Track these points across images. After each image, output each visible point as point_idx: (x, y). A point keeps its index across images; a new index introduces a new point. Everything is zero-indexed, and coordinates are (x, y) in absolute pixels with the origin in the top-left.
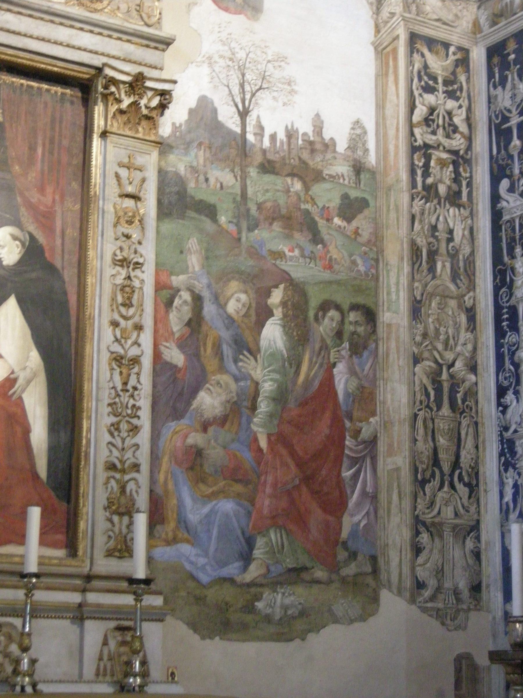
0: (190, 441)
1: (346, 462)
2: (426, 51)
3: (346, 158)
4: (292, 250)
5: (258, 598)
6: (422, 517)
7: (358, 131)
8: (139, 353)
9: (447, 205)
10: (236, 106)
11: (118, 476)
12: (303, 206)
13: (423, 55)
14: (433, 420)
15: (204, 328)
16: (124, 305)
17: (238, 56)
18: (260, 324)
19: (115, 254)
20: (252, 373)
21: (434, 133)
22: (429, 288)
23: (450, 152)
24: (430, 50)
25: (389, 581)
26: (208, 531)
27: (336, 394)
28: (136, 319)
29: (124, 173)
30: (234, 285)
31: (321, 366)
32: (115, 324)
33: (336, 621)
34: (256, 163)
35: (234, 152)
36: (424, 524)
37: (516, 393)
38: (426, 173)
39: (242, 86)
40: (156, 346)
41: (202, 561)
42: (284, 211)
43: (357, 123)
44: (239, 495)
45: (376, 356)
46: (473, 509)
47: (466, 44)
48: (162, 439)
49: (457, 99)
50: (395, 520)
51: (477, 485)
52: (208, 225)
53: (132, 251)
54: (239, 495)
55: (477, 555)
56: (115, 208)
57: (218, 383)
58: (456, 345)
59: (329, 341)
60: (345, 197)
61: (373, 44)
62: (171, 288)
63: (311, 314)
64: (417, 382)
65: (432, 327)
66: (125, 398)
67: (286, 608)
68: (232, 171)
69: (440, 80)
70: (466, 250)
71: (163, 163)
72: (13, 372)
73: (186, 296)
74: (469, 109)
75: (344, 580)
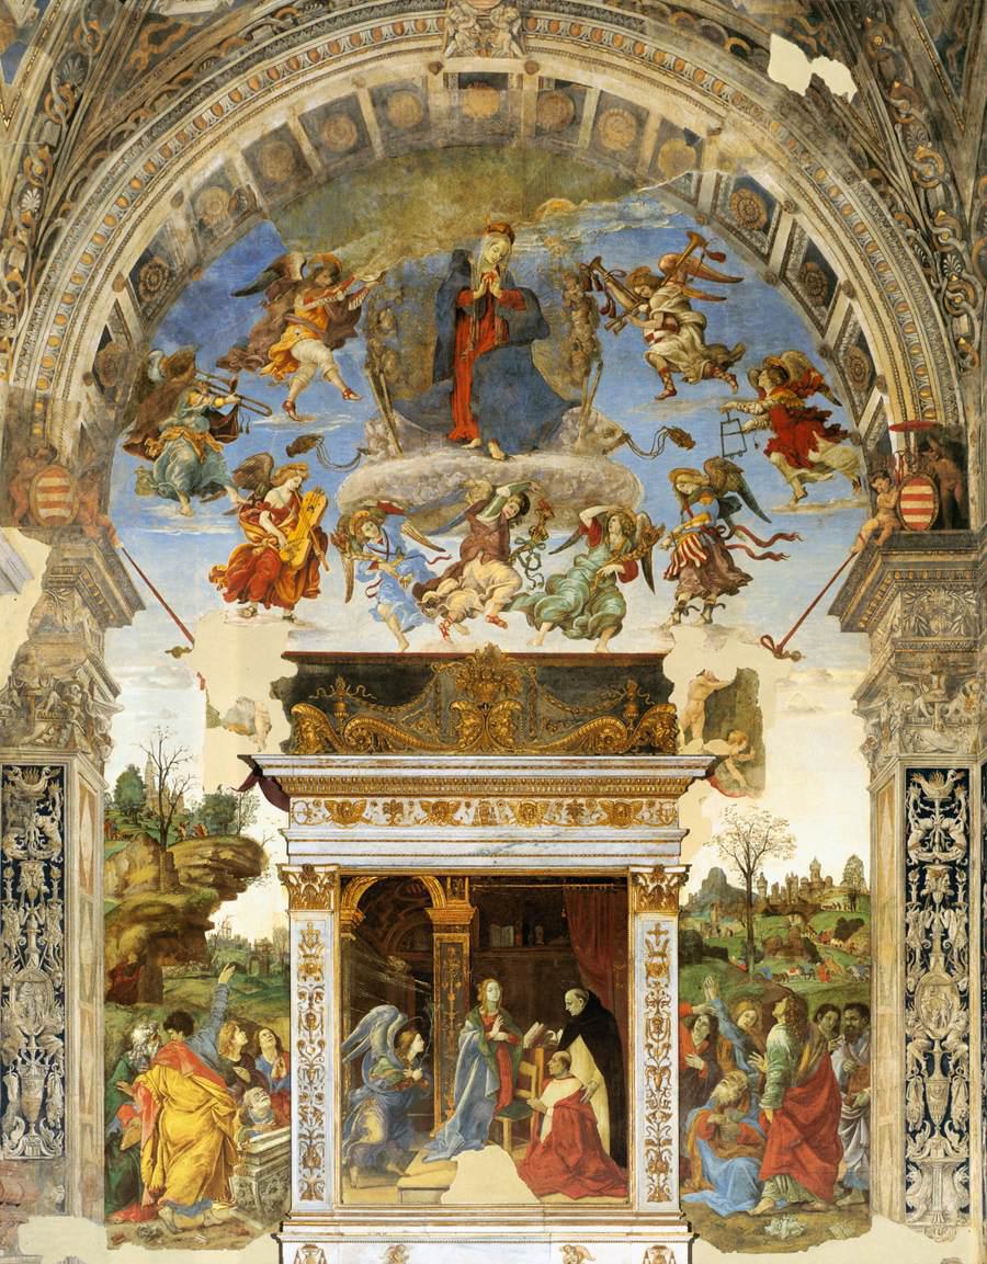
1: (842, 1123)
2: (922, 781)
6: (912, 1159)
7: (854, 866)
13: (919, 786)
15: (720, 1040)
21: (930, 851)
23: (945, 863)
24: (927, 780)
25: (880, 1207)
26: (726, 1182)
28: (666, 1040)
29: (652, 938)
30: (743, 1005)
32: (650, 1046)
33: (833, 1237)
34: (760, 910)
35: (741, 905)
36: (914, 1164)
38: (921, 886)
39: (748, 855)
40: (680, 1058)
41: (720, 1201)
42: (785, 942)
44: (750, 1154)
45: (870, 1041)
46: (962, 1150)
47: (965, 765)
48: (689, 1121)
49: (955, 816)
50: (887, 1161)
51: (968, 1131)
52: (721, 964)
54: (750, 1154)
55: (966, 1185)
57: (732, 1078)
60: (842, 921)
61: (868, 789)
63: (811, 1017)
64: (909, 1056)
66: (658, 1095)
69: (937, 804)
70: (962, 944)
71: (682, 926)
73: (705, 1019)
74: (968, 821)
75: (840, 1209)
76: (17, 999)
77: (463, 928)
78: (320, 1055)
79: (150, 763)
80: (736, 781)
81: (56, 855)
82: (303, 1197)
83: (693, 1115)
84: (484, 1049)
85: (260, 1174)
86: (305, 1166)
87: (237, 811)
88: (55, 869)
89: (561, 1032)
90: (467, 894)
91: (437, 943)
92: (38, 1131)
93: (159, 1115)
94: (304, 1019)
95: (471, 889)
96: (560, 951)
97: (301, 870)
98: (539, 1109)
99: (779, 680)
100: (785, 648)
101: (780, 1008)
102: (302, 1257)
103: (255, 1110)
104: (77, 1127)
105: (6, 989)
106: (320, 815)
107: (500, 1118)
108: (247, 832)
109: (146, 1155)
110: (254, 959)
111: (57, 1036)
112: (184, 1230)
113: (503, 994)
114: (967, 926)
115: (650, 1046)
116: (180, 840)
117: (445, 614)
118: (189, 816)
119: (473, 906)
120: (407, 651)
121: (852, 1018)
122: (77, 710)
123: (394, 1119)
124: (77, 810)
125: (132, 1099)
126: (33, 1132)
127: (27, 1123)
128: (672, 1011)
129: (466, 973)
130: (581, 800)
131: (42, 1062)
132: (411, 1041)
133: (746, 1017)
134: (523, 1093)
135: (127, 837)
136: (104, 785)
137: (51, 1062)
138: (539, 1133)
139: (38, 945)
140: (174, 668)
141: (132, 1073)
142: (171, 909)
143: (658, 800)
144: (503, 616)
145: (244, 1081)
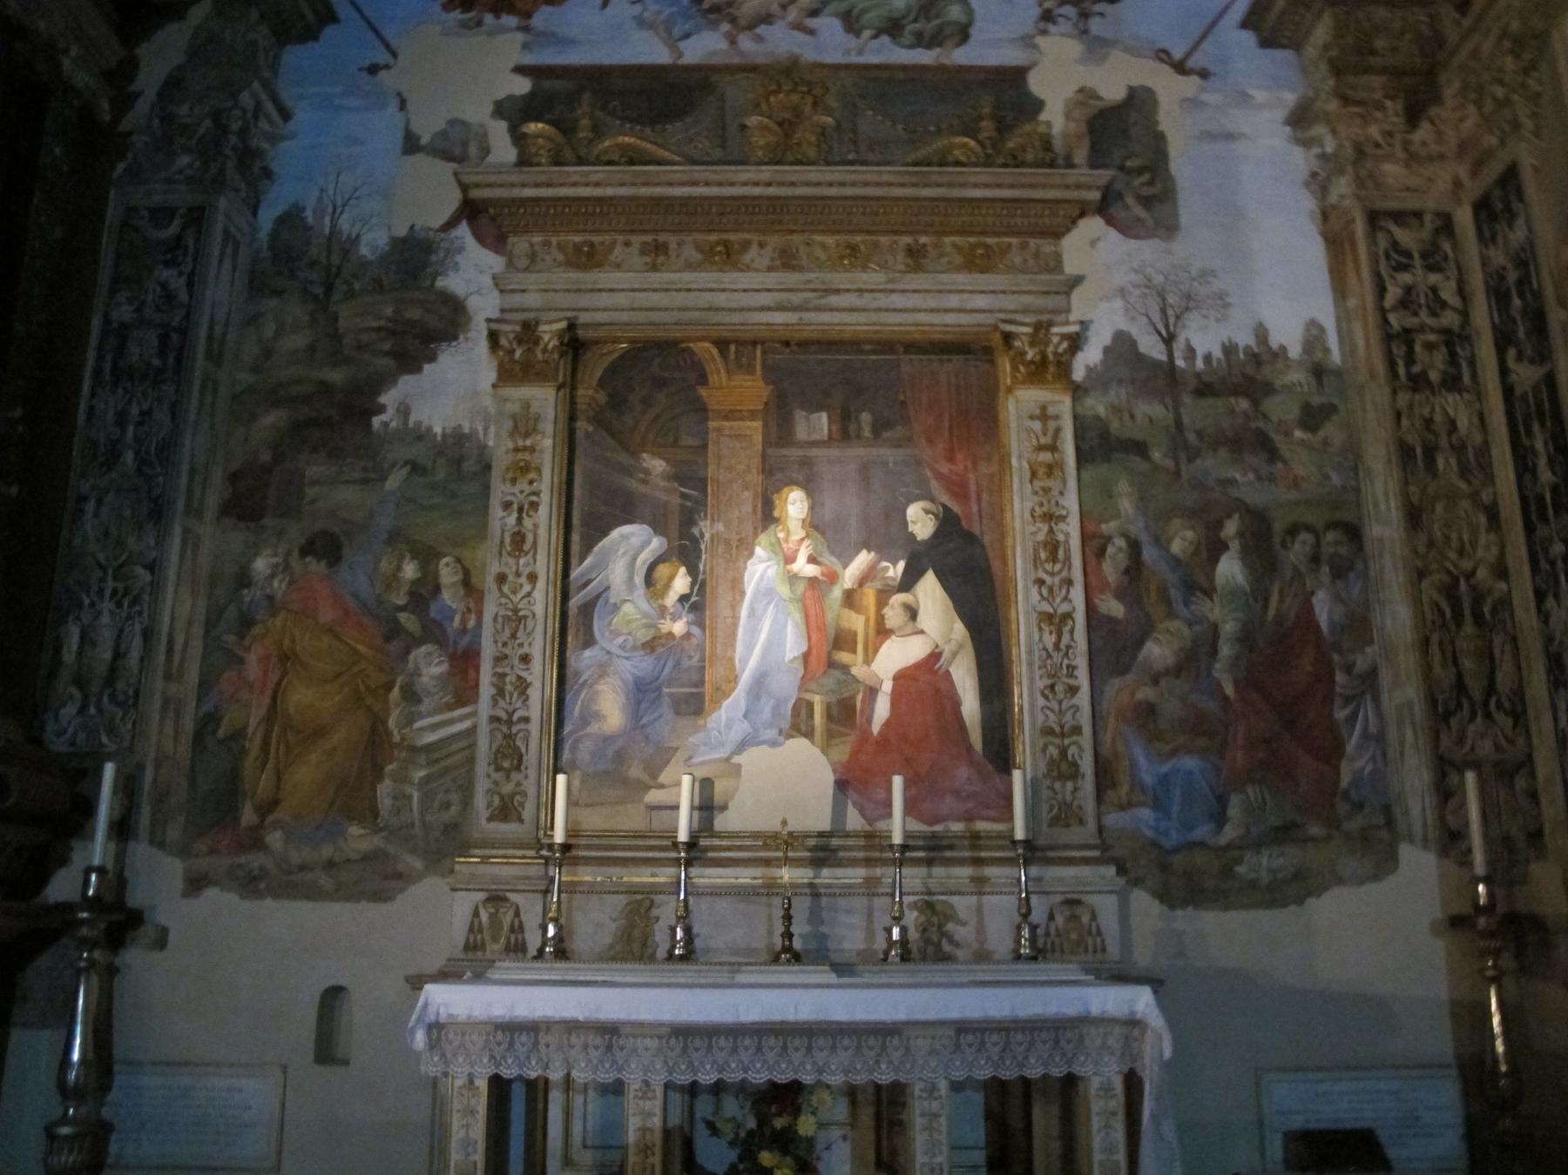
0: (1140, 696)
1: (1338, 701)
3: (1300, 363)
4: (1245, 474)
5: (1240, 861)
7: (1314, 331)
8: (1070, 609)
9: (1444, 392)
10: (1160, 334)
11: (1057, 741)
12: (1253, 425)
13: (1389, 232)
14: (1453, 642)
16: (1047, 561)
17: (1155, 282)
18: (1214, 560)
19: (1033, 510)
20: (1210, 615)
21: (1415, 314)
22: (1431, 490)
24: (1396, 223)
27: (1318, 626)
28: (1064, 574)
29: (1037, 426)
30: (1176, 523)
31: (1296, 595)
32: (1041, 582)
33: (1340, 881)
36: (1452, 763)
37: (1556, 596)
38: (1410, 359)
39: (1163, 311)
43: (1313, 324)
46: (1521, 741)
51: (1524, 711)
53: (1053, 502)
55: (1533, 795)
56: (1029, 463)
57: (1168, 631)
58: (1474, 551)
59: (1302, 569)
62: (1102, 536)
64: (1425, 599)
65: (1439, 534)
66: (1057, 657)
67: (1274, 871)
68: (1164, 403)
69: (1416, 255)
70: (1477, 438)
71: (1079, 409)
72: (937, 646)
73: (1120, 542)
76: (96, 515)
77: (753, 415)
78: (529, 594)
79: (320, 199)
80: (1139, 219)
81: (177, 319)
82: (490, 819)
83: (1114, 687)
84: (784, 590)
85: (427, 780)
86: (498, 769)
87: (434, 258)
88: (175, 336)
89: (901, 565)
90: (758, 367)
91: (712, 436)
92: (100, 710)
93: (279, 683)
94: (507, 540)
95: (764, 361)
96: (898, 446)
97: (518, 328)
98: (871, 683)
99: (1186, 100)
100: (1190, 64)
101: (1231, 528)
102: (484, 917)
103: (425, 679)
104: (157, 703)
105: (83, 499)
106: (548, 258)
107: (808, 696)
108: (441, 283)
109: (254, 747)
110: (440, 453)
111: (144, 567)
112: (302, 868)
113: (812, 508)
114: (1481, 417)
115: (1041, 582)
116: (351, 295)
117: (733, 20)
118: (365, 264)
119: (767, 384)
120: (680, 62)
121: (1337, 543)
122: (233, 139)
123: (642, 694)
124: (215, 262)
125: (241, 661)
126: (92, 710)
127: (86, 696)
128: (1071, 530)
129: (755, 478)
130: (923, 239)
131: (119, 605)
132: (672, 578)
133: (1182, 541)
134: (844, 657)
135: (279, 293)
136: (254, 229)
137: (132, 604)
138: (869, 721)
139: (136, 438)
140: (368, 88)
141: (246, 622)
142: (325, 388)
143: (1033, 242)
144: (812, 23)
145: (409, 634)
